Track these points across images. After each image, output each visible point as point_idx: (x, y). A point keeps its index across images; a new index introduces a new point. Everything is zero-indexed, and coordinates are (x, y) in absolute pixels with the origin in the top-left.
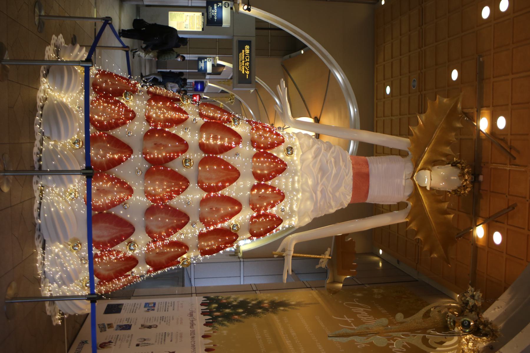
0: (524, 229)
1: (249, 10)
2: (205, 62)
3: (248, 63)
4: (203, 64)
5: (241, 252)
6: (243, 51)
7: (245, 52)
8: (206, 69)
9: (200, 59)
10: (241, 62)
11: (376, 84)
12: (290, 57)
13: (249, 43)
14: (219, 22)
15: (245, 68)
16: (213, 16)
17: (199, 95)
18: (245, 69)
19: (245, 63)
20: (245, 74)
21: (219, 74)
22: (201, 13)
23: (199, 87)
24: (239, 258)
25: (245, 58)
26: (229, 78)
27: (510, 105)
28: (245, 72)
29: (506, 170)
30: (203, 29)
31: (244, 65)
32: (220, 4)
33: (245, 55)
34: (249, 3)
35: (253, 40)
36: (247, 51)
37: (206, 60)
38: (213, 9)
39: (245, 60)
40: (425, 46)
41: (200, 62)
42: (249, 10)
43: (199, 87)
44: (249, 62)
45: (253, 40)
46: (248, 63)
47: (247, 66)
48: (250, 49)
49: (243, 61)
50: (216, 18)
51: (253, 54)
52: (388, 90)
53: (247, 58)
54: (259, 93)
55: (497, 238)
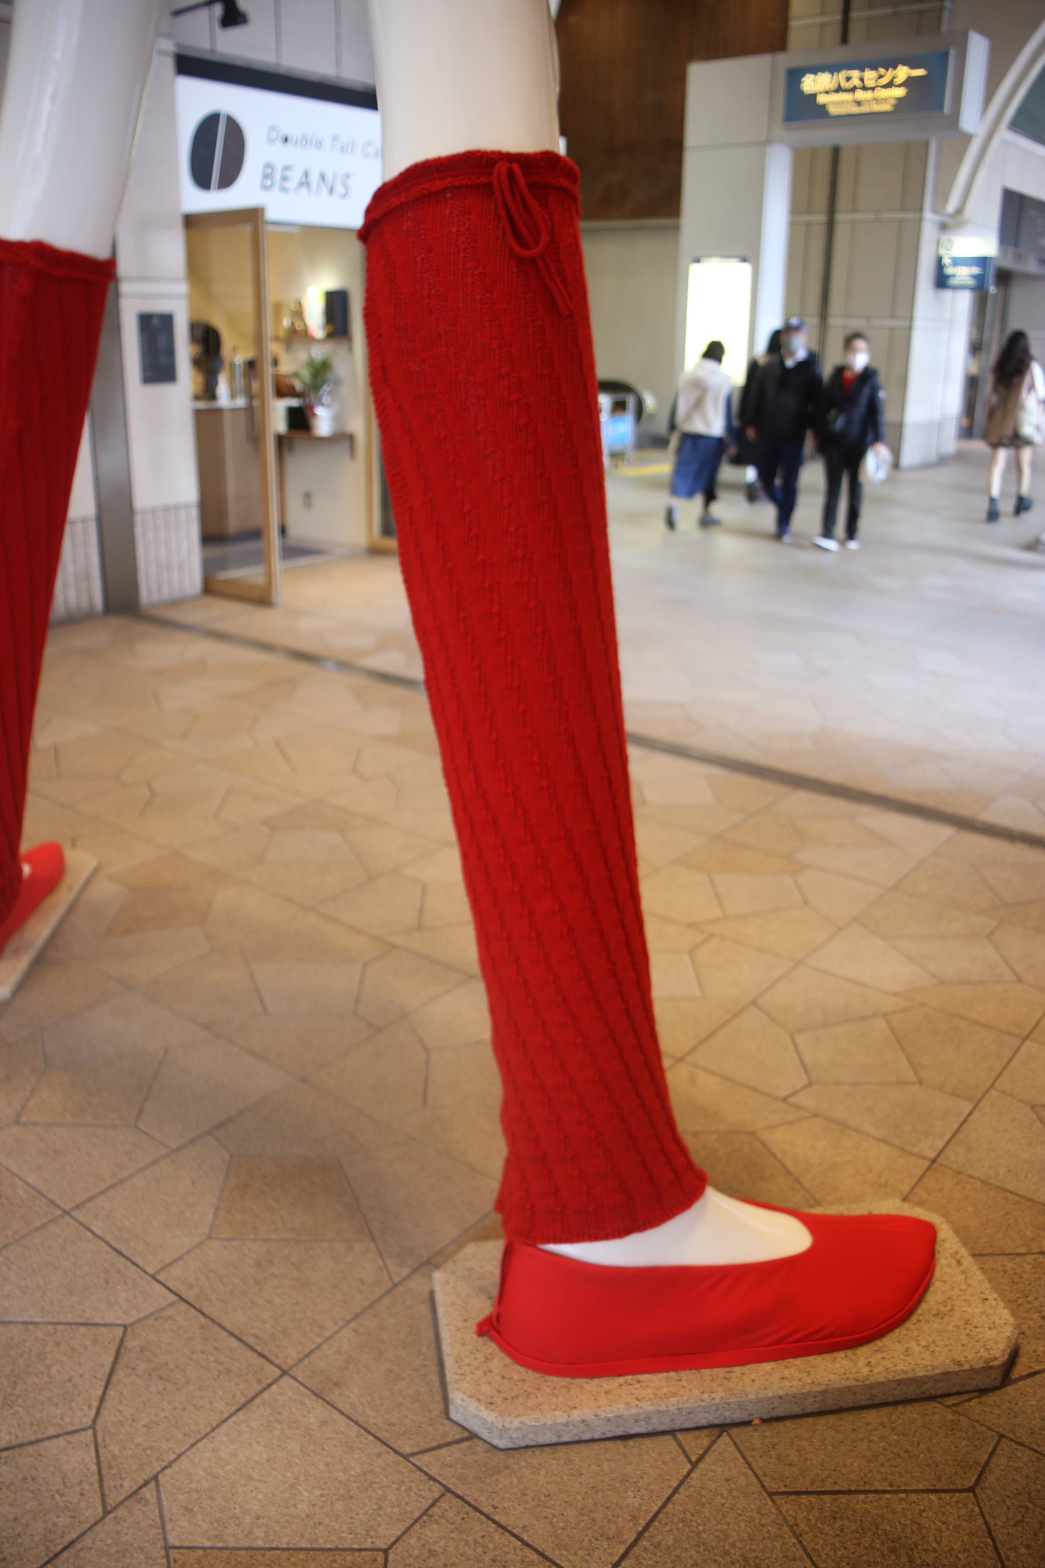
2: (956, 262)
6: (822, 99)
8: (983, 262)
10: (859, 103)
13: (795, 76)
18: (890, 85)
19: (864, 88)
20: (909, 82)
25: (846, 91)
28: (899, 86)
31: (873, 89)
33: (839, 89)
37: (946, 261)
45: (784, 61)
47: (881, 77)
48: (815, 70)
49: (860, 95)
53: (848, 79)
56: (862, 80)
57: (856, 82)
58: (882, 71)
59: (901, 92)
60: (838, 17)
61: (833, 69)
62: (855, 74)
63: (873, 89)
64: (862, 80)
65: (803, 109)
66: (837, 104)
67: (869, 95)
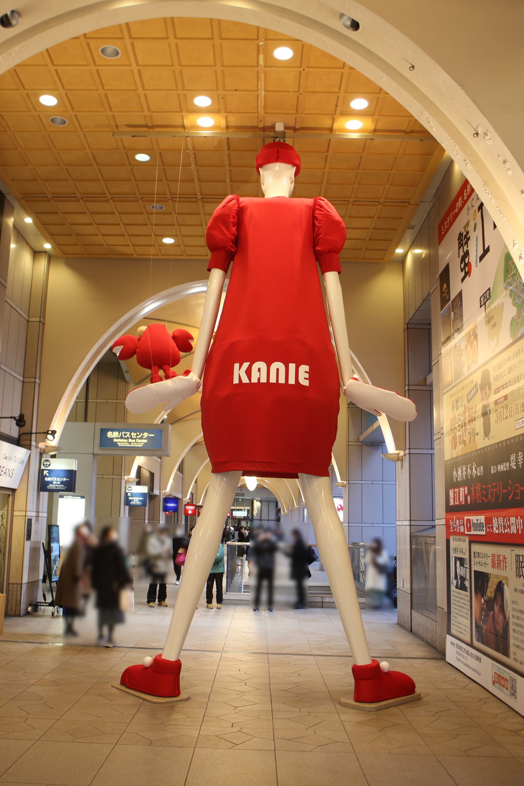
0: (342, 74)
1: (54, 433)
3: (132, 434)
4: (134, 498)
5: (397, 452)
6: (115, 440)
7: (117, 438)
8: (143, 495)
9: (127, 502)
10: (130, 443)
11: (160, 257)
12: (127, 372)
13: (104, 431)
14: (71, 474)
15: (139, 439)
16: (62, 483)
17: (186, 505)
18: (141, 438)
19: (132, 439)
20: (148, 438)
21: (152, 475)
22: (60, 499)
23: (172, 505)
24: (405, 455)
25: (125, 438)
26: (159, 460)
27: (178, 92)
28: (145, 439)
29: (265, 96)
30: (82, 497)
31: (135, 439)
32: (45, 472)
33: (121, 438)
34: (45, 433)
35: (99, 426)
36: (116, 434)
37: (129, 494)
38: (51, 482)
39: (128, 438)
40: (105, 194)
41: (132, 503)
42: (54, 433)
43: (172, 505)
44: (131, 433)
45: (99, 426)
46: (132, 434)
47: (137, 435)
48: (113, 430)
49: (130, 440)
50: (65, 479)
51: (120, 426)
52: (168, 241)
53: (125, 435)
54: (182, 417)
55: (359, 104)
56: (131, 436)
57: (128, 435)
58: (138, 433)
59: (146, 441)
60: (84, 400)
61: (119, 431)
62: (129, 433)
63: (135, 439)
64: (130, 435)
65: (106, 442)
66: (122, 443)
67: (134, 441)
